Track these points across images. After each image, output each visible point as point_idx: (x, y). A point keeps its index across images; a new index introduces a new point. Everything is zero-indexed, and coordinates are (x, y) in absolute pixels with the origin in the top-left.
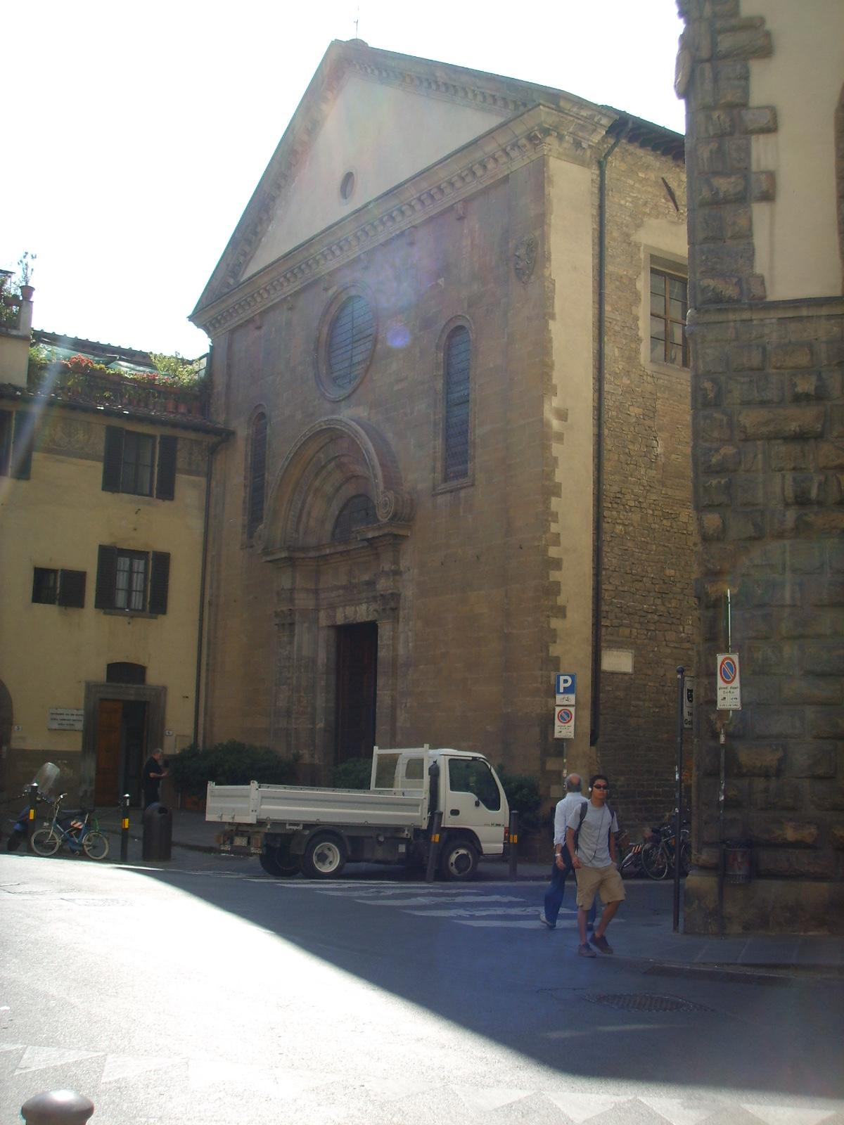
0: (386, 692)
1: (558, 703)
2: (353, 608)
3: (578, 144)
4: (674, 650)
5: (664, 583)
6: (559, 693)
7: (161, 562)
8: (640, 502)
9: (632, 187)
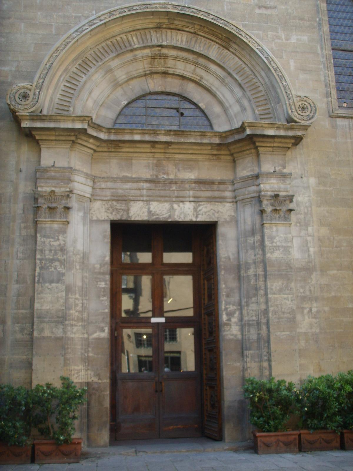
0: (286, 296)
2: (167, 205)
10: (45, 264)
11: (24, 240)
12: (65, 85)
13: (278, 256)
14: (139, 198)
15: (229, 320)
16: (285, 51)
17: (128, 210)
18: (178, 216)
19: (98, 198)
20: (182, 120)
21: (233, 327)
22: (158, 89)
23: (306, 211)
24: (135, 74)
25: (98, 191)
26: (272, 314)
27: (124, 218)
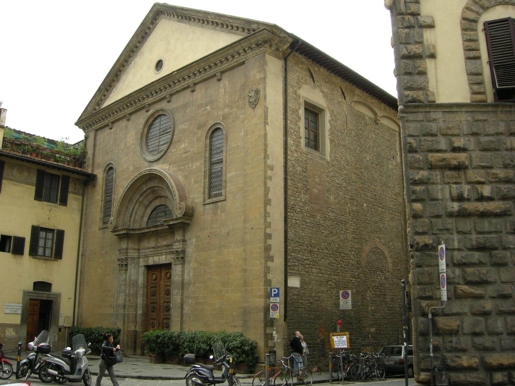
1: (271, 301)
2: (158, 257)
3: (277, 49)
4: (316, 277)
5: (311, 247)
6: (271, 296)
7: (61, 234)
8: (301, 210)
9: (297, 71)
24: (150, 200)
25: (141, 254)
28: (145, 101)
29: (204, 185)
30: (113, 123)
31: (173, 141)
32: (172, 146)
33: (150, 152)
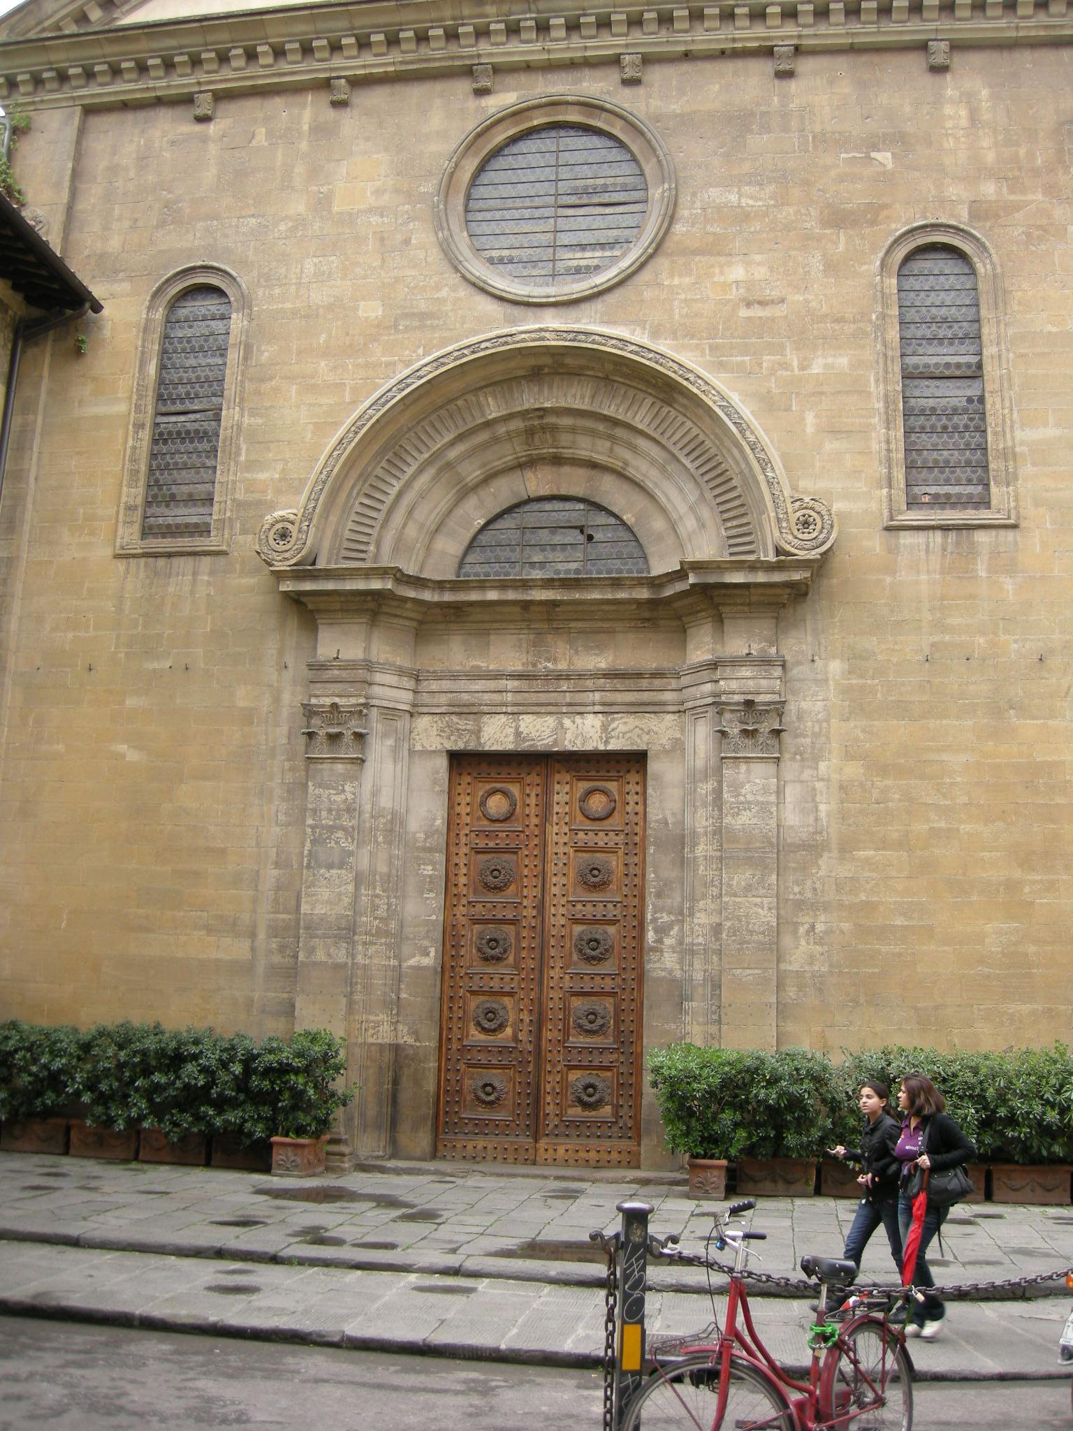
0: (759, 900)
2: (551, 721)
10: (320, 834)
11: (288, 791)
12: (361, 503)
13: (748, 822)
14: (499, 709)
15: (660, 941)
16: (796, 394)
17: (479, 731)
18: (570, 741)
19: (425, 710)
20: (589, 550)
21: (666, 955)
22: (544, 491)
23: (817, 729)
24: (498, 464)
25: (425, 698)
26: (727, 935)
27: (472, 746)
28: (484, 47)
29: (889, 450)
30: (222, 96)
31: (669, 245)
32: (662, 263)
33: (491, 261)
